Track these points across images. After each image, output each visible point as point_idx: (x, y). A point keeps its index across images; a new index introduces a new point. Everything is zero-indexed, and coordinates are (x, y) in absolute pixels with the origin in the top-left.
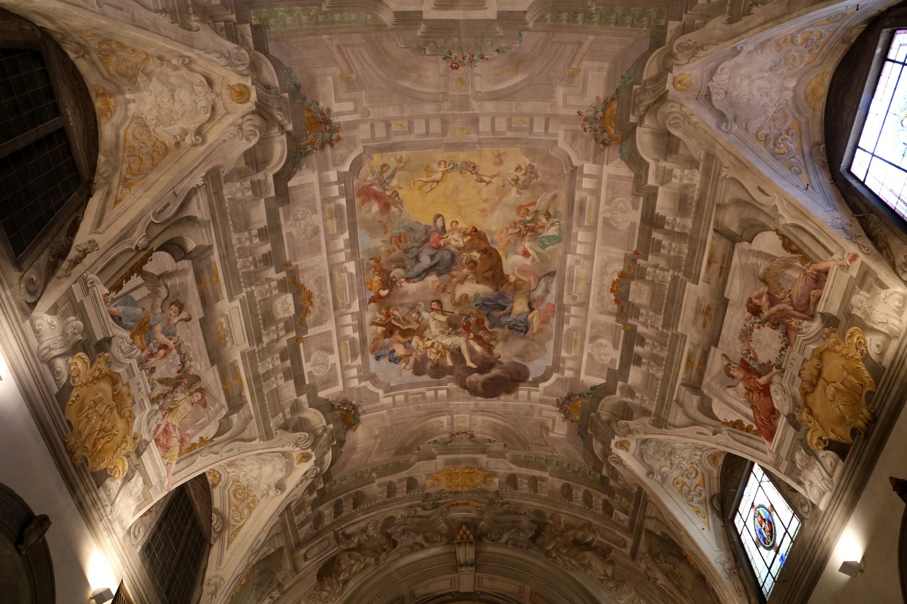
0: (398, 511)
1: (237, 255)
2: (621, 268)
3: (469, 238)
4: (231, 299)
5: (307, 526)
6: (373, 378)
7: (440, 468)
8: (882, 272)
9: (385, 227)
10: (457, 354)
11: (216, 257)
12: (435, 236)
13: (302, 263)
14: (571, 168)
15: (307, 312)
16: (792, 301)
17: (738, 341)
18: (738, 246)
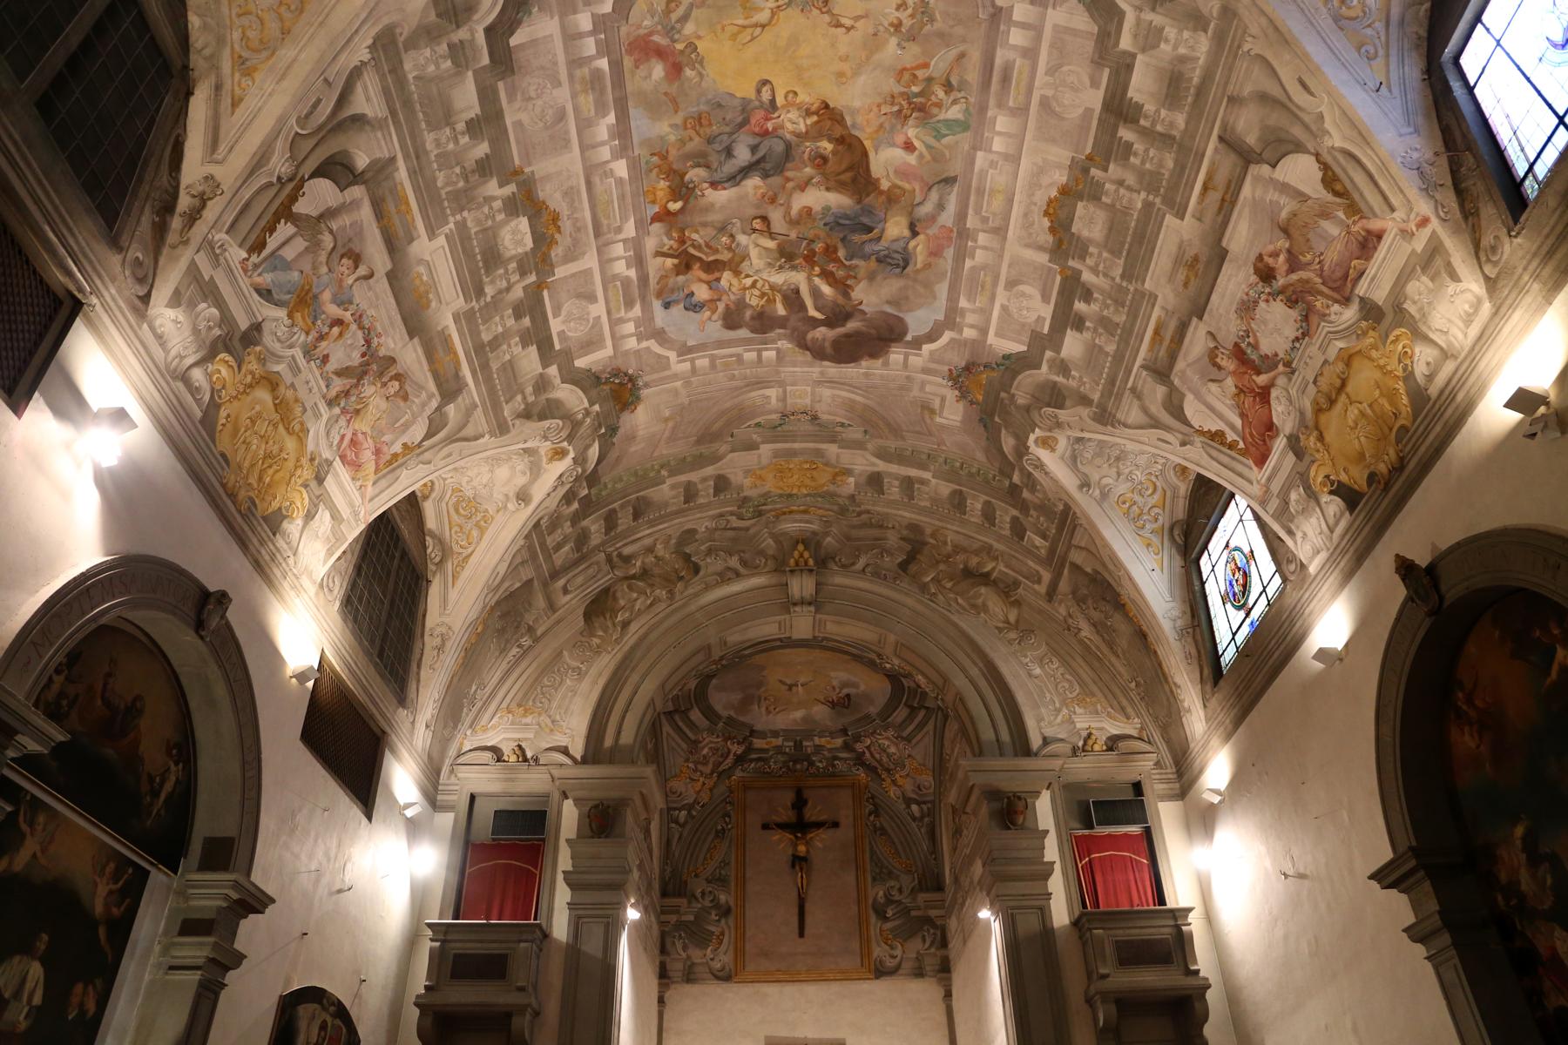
0: (701, 522)
1: (435, 166)
2: (1064, 179)
3: (815, 118)
4: (432, 235)
5: (567, 548)
6: (660, 335)
7: (765, 461)
8: (1457, 252)
9: (674, 102)
10: (793, 298)
11: (402, 174)
12: (758, 116)
13: (540, 168)
14: (991, 10)
15: (552, 242)
16: (1322, 270)
17: (1233, 316)
18: (1254, 170)
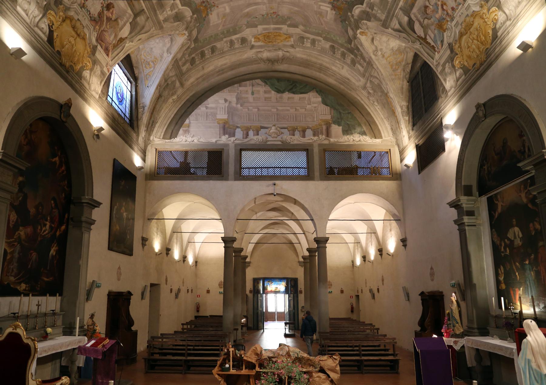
18: (133, 16)
